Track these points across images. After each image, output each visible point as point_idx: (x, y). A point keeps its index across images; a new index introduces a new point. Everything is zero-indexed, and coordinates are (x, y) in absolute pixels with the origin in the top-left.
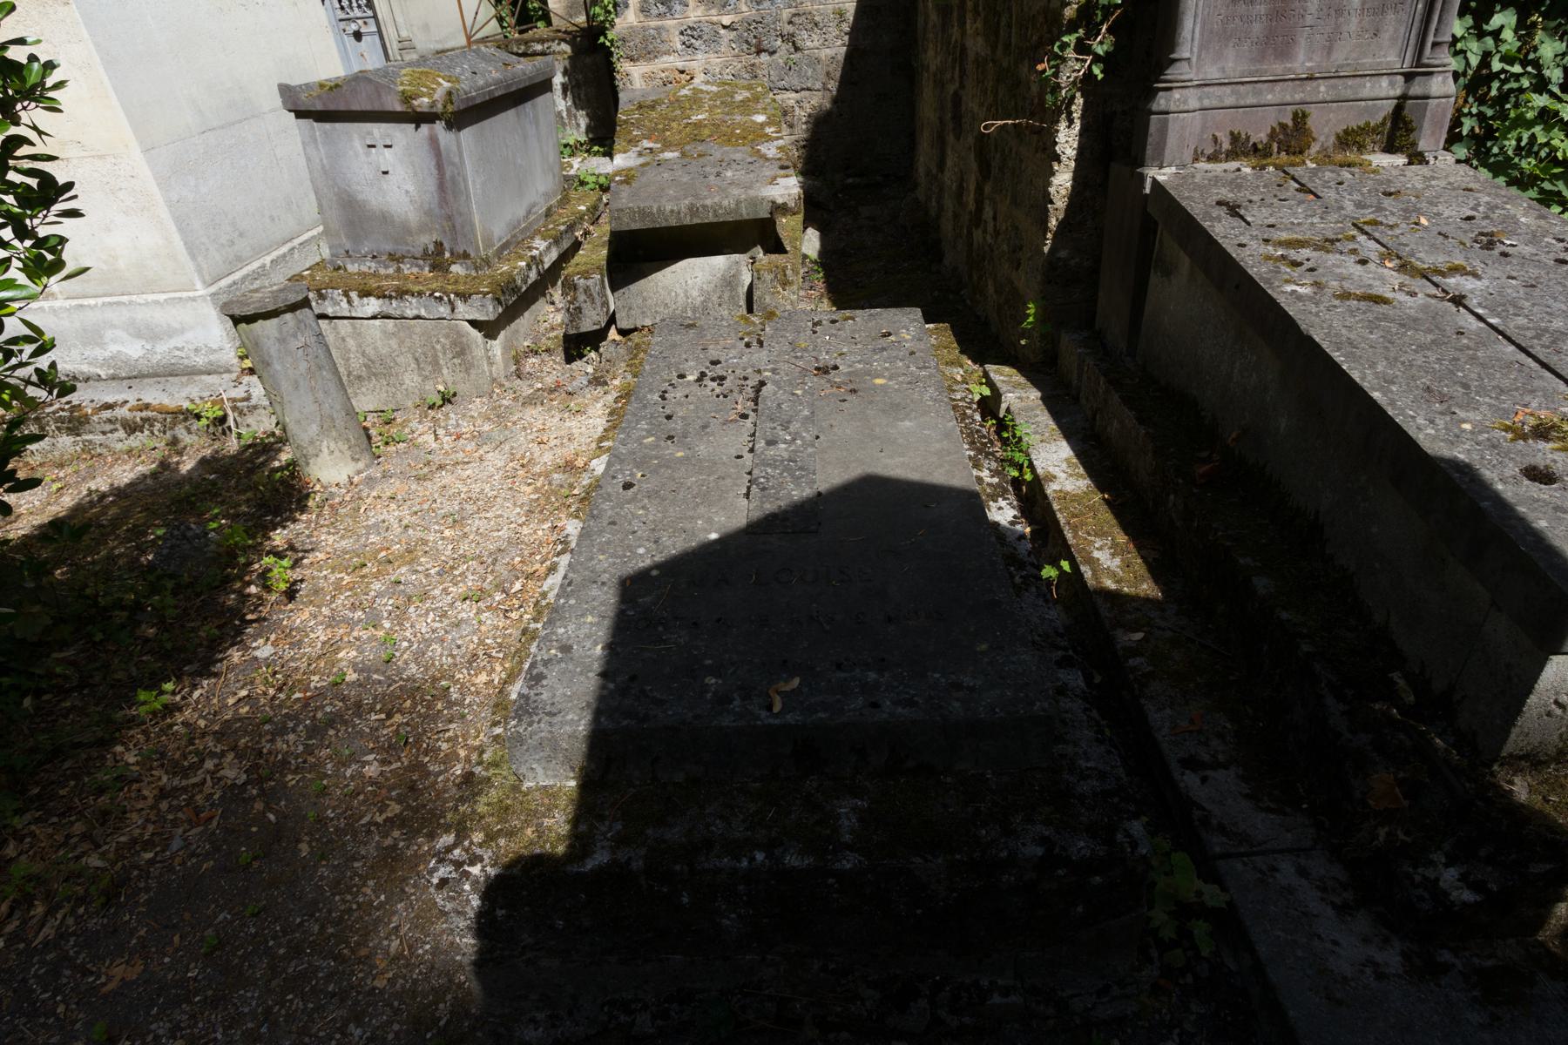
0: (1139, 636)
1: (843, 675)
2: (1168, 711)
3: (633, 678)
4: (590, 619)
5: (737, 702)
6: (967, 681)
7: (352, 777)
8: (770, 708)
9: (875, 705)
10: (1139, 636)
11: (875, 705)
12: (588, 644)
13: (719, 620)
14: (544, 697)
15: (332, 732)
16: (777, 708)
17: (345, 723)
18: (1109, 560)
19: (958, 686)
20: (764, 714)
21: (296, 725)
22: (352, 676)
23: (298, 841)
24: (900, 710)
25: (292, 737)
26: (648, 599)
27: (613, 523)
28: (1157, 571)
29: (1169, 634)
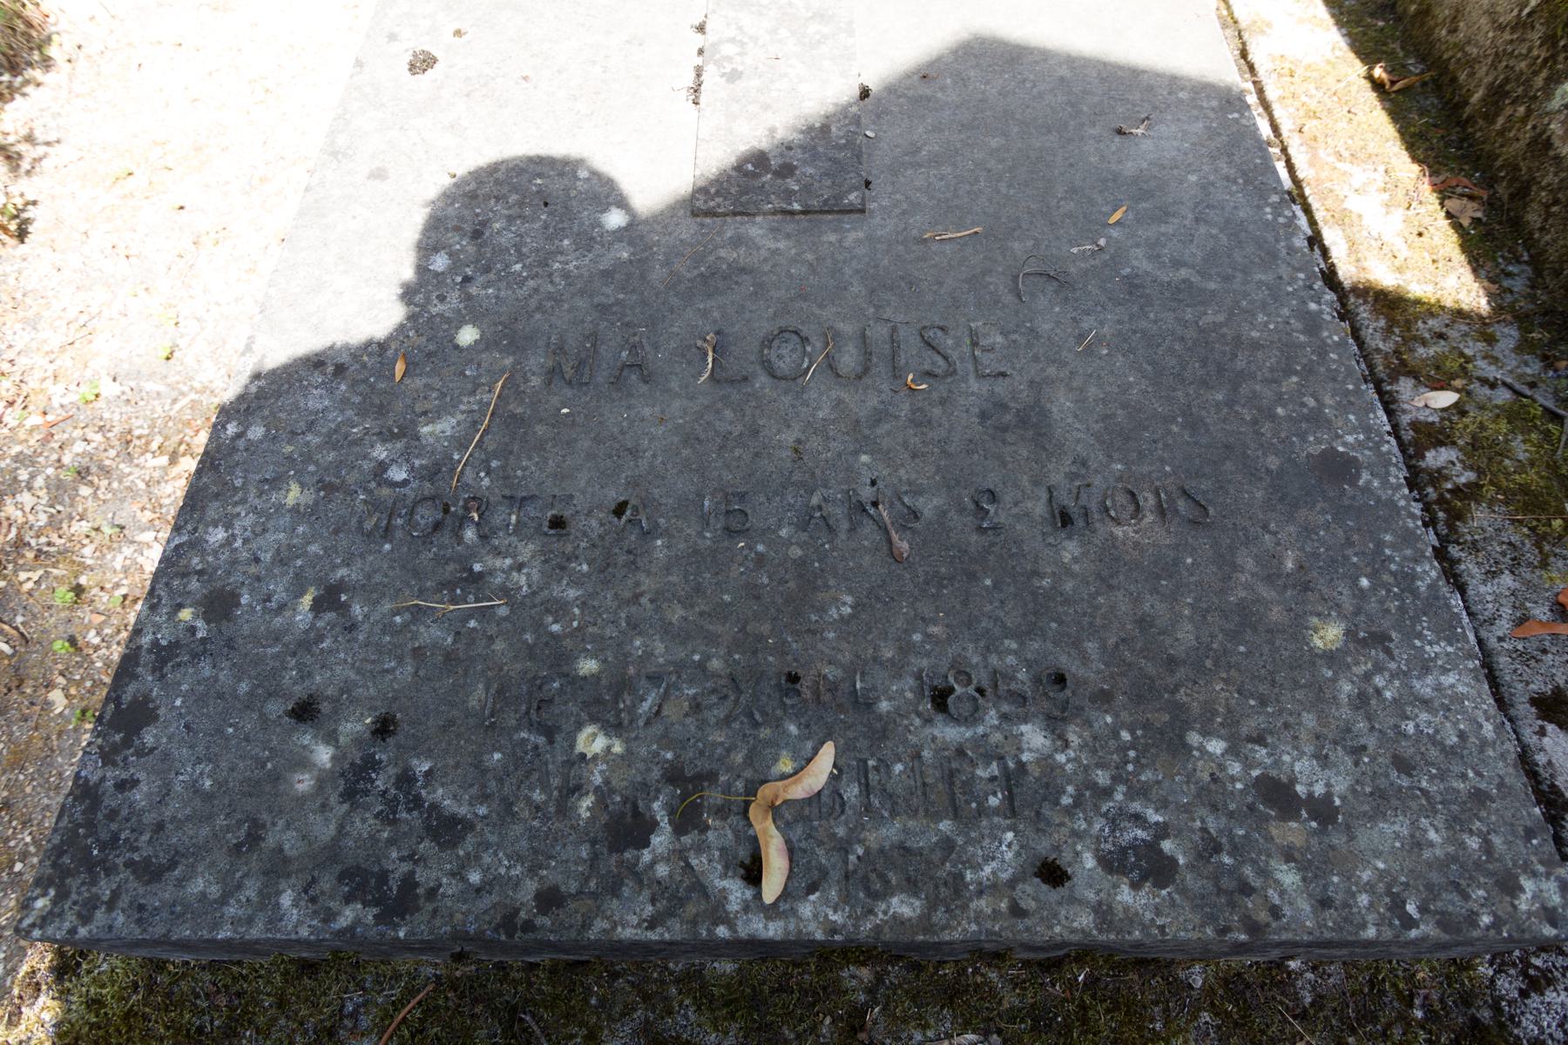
0: (1446, 399)
1: (950, 733)
2: (1507, 580)
3: (384, 728)
4: (294, 495)
5: (661, 840)
6: (1309, 778)
7: (126, 570)
8: (753, 874)
9: (1053, 874)
10: (1446, 399)
11: (1053, 874)
12: (279, 589)
13: (619, 510)
14: (138, 796)
15: (85, 491)
16: (772, 887)
17: (106, 472)
18: (1391, 226)
19: (1277, 794)
20: (736, 892)
21: (33, 477)
22: (109, 389)
23: (50, 686)
24: (1125, 895)
25: (26, 498)
26: (446, 426)
27: (379, 174)
28: (1483, 245)
29: (1502, 396)
